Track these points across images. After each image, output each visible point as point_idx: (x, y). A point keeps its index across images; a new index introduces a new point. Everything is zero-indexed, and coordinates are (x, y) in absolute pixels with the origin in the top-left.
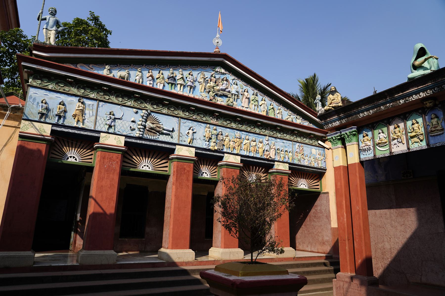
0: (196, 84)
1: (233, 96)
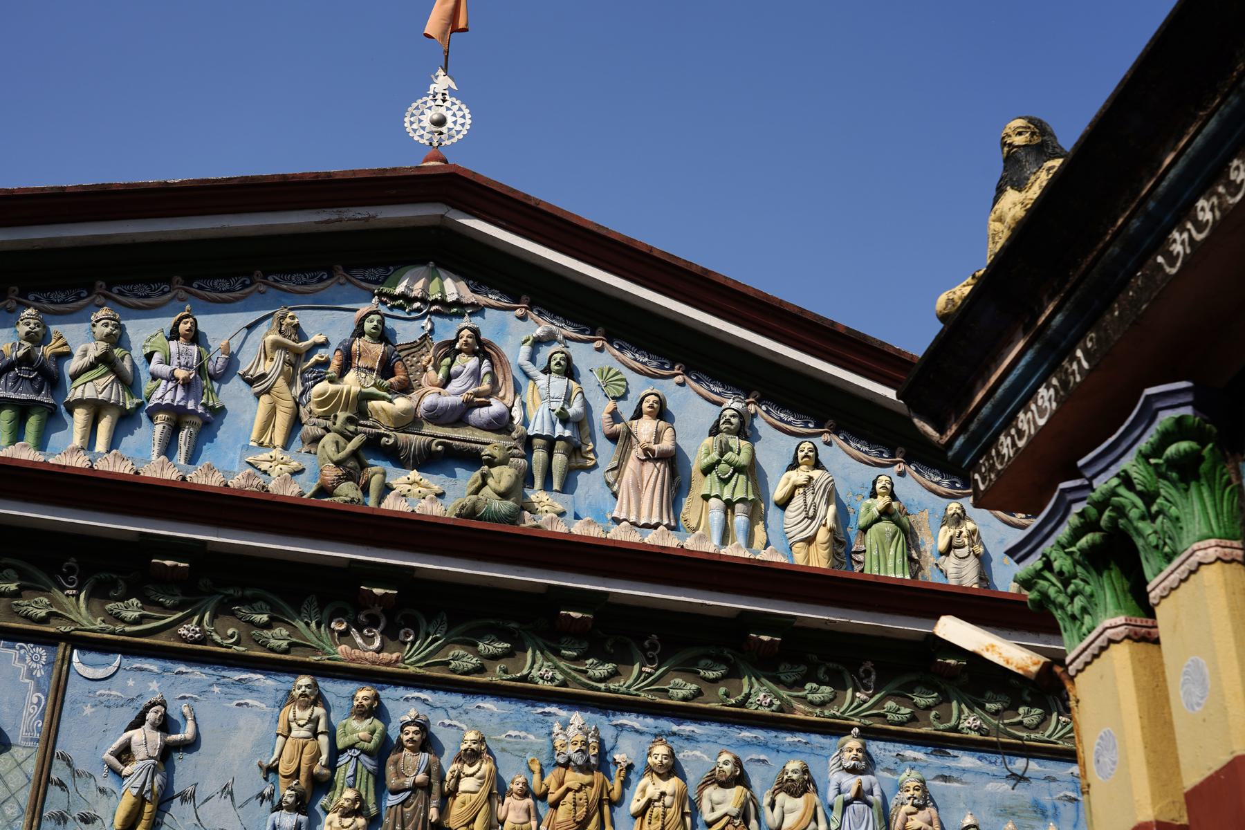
0: (232, 394)
1: (539, 455)
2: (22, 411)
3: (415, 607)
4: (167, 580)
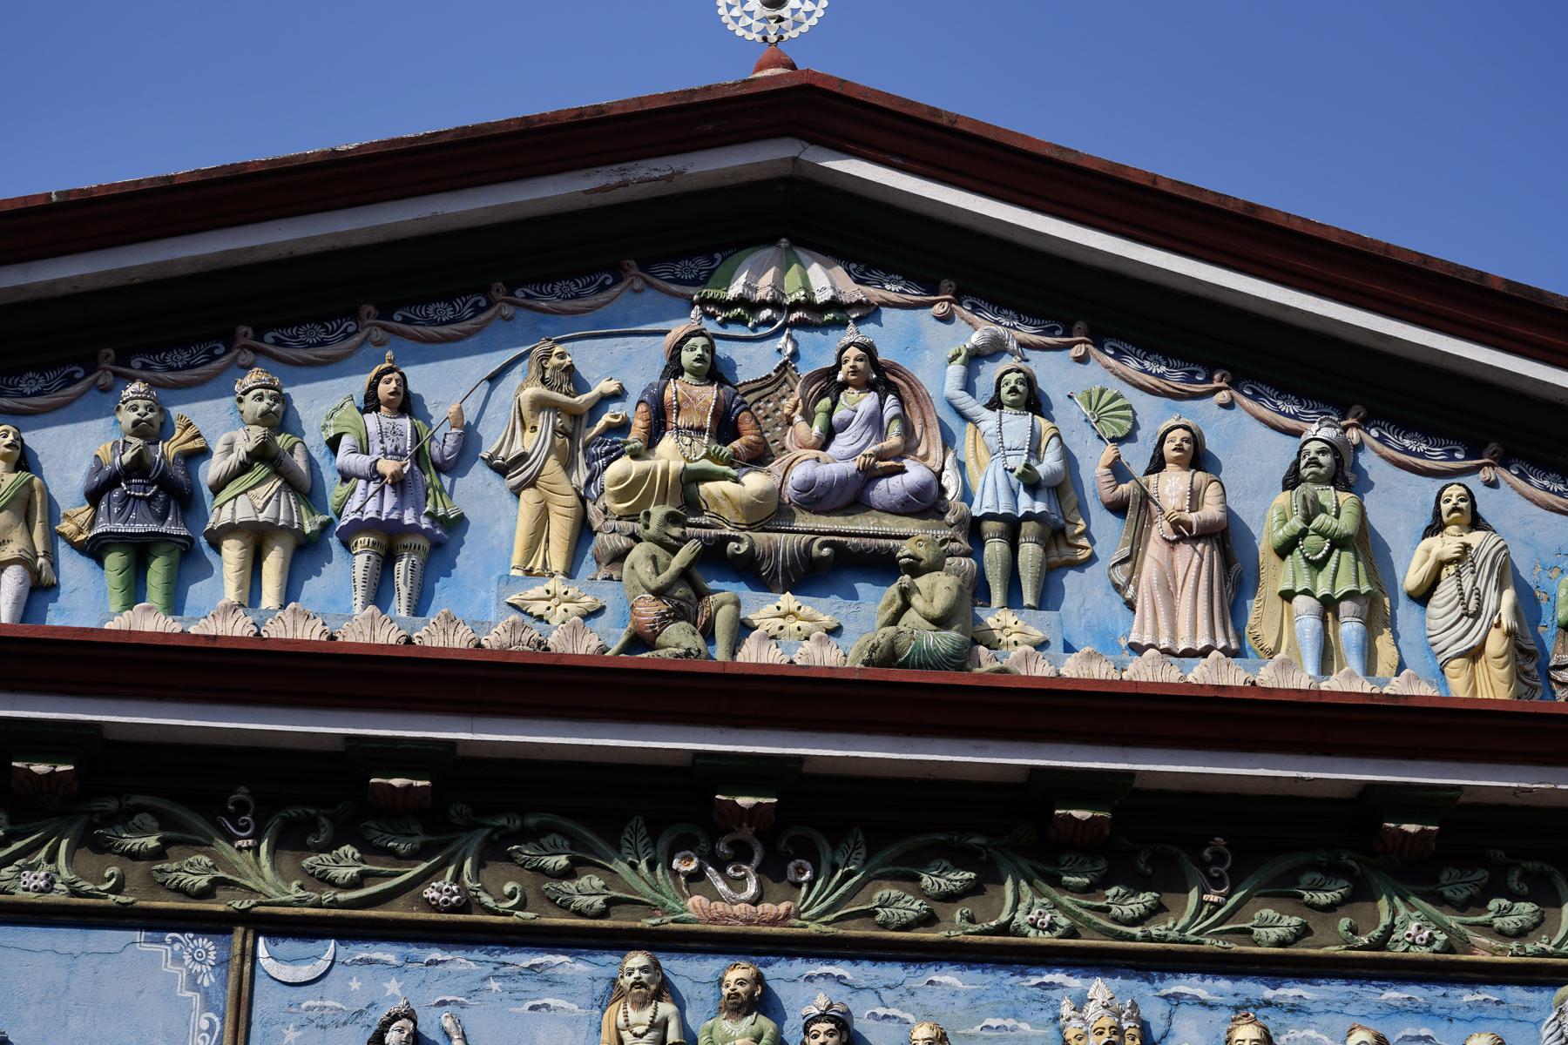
0: (474, 492)
1: (995, 549)
2: (140, 551)
3: (810, 822)
4: (397, 810)
